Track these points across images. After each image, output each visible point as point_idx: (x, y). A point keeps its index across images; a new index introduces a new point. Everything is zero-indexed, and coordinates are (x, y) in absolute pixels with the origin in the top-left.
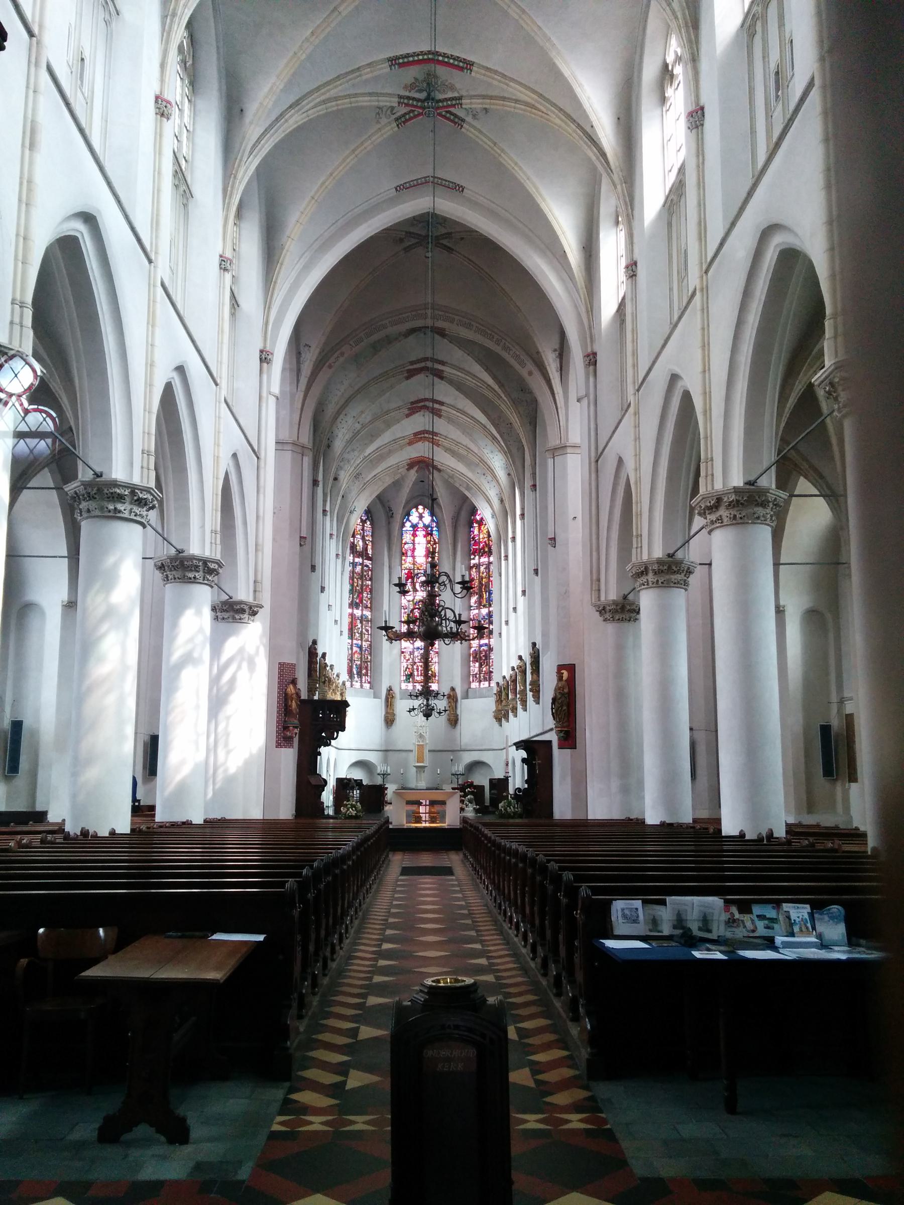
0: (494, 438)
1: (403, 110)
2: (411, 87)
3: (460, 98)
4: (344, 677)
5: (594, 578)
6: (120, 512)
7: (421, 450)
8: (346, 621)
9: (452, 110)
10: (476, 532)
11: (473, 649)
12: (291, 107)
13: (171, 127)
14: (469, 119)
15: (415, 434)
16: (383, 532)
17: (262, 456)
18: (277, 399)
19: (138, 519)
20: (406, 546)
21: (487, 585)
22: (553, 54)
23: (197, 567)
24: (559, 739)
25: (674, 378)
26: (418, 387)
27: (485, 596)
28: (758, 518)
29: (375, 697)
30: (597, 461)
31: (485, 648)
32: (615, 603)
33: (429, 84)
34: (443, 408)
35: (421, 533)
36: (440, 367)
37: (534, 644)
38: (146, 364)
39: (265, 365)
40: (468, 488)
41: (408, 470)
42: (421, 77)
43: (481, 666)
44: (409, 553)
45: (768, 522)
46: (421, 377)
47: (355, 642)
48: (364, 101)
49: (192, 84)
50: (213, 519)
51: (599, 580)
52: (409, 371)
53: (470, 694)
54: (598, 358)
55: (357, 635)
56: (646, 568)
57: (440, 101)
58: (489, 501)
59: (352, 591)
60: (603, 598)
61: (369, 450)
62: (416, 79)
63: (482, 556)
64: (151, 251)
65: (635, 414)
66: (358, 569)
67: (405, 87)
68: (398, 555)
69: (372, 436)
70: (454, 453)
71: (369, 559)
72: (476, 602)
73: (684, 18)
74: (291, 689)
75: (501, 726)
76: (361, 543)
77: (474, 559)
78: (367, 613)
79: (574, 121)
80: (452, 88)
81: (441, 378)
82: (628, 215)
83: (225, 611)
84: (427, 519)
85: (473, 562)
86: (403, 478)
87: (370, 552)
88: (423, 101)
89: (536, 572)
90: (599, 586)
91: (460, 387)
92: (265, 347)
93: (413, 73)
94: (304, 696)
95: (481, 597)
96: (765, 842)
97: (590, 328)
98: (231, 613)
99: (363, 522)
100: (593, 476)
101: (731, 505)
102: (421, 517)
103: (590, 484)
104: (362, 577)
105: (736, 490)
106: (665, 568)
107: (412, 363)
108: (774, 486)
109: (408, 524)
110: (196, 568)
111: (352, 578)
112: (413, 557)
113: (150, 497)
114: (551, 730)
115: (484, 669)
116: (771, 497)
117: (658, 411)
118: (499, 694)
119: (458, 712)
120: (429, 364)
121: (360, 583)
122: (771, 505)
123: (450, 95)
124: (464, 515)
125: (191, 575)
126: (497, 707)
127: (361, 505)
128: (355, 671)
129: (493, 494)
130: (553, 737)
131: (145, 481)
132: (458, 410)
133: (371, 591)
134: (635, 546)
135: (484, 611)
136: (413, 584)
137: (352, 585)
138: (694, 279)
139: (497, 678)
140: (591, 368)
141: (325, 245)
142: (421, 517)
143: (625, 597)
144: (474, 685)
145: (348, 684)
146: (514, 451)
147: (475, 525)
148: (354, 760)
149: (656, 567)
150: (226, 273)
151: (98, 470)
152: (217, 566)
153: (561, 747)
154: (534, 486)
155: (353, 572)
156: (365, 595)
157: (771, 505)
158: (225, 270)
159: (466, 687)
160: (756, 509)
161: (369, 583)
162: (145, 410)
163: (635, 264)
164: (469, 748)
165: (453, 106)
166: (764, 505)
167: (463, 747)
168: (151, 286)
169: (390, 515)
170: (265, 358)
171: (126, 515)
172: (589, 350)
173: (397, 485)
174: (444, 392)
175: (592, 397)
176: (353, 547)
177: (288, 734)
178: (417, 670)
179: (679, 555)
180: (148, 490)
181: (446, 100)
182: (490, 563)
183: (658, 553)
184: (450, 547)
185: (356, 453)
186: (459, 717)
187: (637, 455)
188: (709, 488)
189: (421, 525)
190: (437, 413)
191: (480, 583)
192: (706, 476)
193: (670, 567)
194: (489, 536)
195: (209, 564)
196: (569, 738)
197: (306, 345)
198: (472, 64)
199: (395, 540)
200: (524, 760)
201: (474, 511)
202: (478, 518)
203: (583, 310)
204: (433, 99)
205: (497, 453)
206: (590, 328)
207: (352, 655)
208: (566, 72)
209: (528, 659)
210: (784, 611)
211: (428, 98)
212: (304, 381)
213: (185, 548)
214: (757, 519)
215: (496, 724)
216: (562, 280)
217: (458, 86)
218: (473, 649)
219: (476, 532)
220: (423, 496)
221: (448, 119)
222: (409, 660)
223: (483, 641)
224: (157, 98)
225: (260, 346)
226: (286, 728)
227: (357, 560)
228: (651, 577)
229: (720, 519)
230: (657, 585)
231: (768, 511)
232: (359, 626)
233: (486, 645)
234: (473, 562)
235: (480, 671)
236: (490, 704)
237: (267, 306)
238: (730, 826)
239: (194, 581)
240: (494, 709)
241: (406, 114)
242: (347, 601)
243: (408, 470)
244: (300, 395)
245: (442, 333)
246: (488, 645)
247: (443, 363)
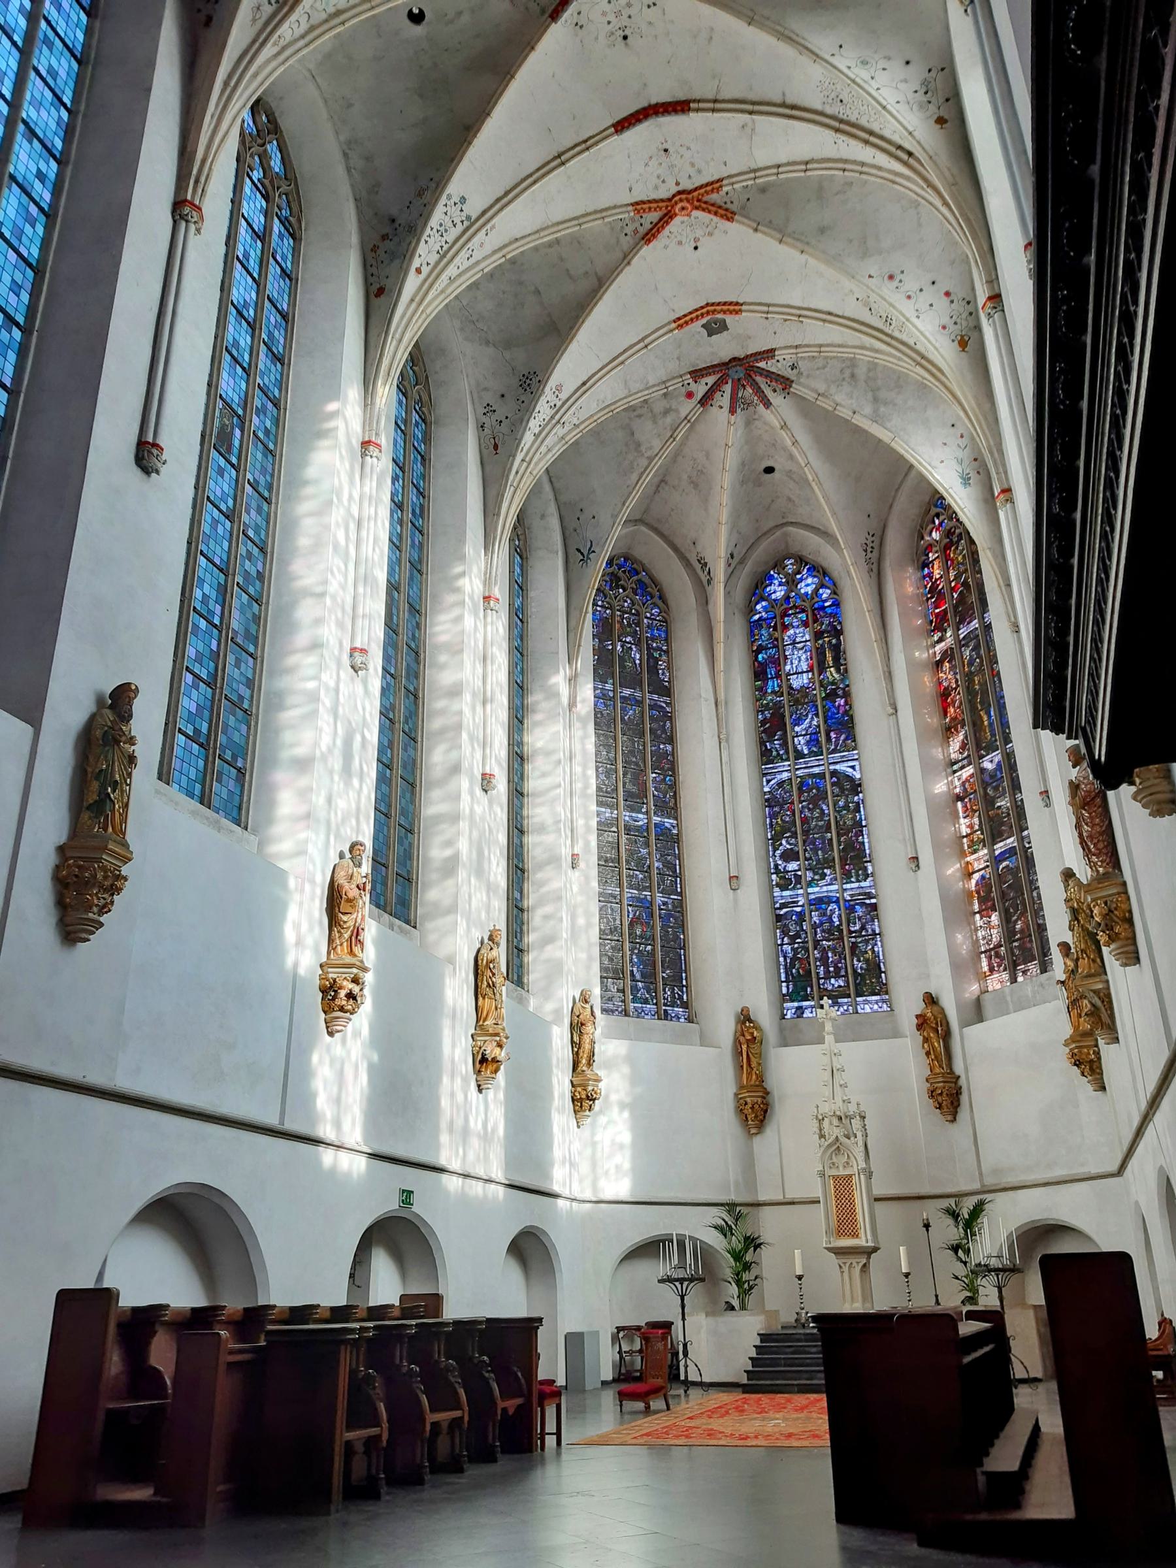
10: (937, 573)
11: (976, 876)
29: (704, 1041)
43: (1007, 919)
44: (771, 671)
63: (961, 622)
72: (963, 747)
75: (1103, 1088)
77: (941, 640)
115: (1018, 927)
119: (959, 1068)
126: (1076, 1028)
142: (792, 582)
148: (637, 1237)
164: (1011, 1180)
167: (990, 1181)
178: (824, 960)
186: (962, 1082)
205: (881, 65)
215: (1083, 1086)
218: (976, 876)
222: (797, 936)
223: (999, 848)
233: (1011, 852)
235: (1009, 932)
240: (1068, 1031)
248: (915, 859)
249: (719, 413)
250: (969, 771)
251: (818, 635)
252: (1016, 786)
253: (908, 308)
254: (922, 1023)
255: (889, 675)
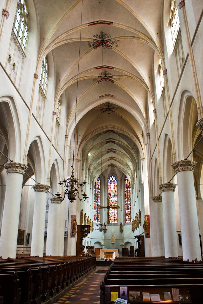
0: (129, 158)
1: (99, 79)
2: (101, 74)
3: (113, 76)
4: (93, 220)
5: (152, 190)
6: (16, 171)
7: (112, 162)
8: (94, 205)
9: (111, 79)
10: (126, 182)
12: (71, 79)
13: (38, 82)
14: (115, 81)
15: (110, 158)
16: (103, 183)
17: (65, 161)
18: (69, 147)
19: (22, 173)
20: (109, 186)
21: (130, 196)
22: (133, 64)
23: (43, 187)
24: (146, 235)
25: (166, 135)
26: (109, 146)
27: (129, 199)
28: (189, 169)
30: (151, 160)
31: (129, 212)
32: (157, 197)
33: (105, 74)
34: (116, 151)
35: (112, 183)
36: (114, 141)
37: (140, 210)
38: (27, 134)
39: (66, 139)
40: (124, 171)
41: (109, 167)
42: (103, 72)
43: (128, 217)
44: (110, 188)
45: (192, 170)
46: (110, 143)
47: (96, 211)
48: (90, 78)
49: (48, 75)
50: (48, 176)
51: (153, 191)
52: (106, 142)
53: (126, 224)
54: (150, 134)
55: (96, 209)
56: (163, 186)
57: (108, 77)
58: (129, 174)
59: (95, 198)
60: (154, 196)
61: (98, 162)
62: (102, 72)
64: (30, 107)
65: (158, 146)
66: (97, 192)
67: (99, 74)
68: (107, 189)
69: (99, 158)
70: (120, 163)
71: (99, 190)
73: (160, 51)
74: (74, 222)
76: (97, 186)
78: (99, 203)
79: (139, 78)
80: (111, 74)
81: (115, 143)
82: (153, 99)
83: (54, 200)
84: (114, 179)
85: (126, 190)
86: (107, 169)
87: (100, 188)
88: (104, 77)
89: (140, 191)
90: (153, 193)
91: (119, 145)
92: (66, 134)
93: (101, 71)
94: (79, 223)
95: (128, 199)
96: (194, 262)
97: (148, 127)
98: (56, 201)
99: (98, 180)
100: (150, 164)
101: (181, 165)
102: (112, 179)
103: (149, 166)
104: (98, 194)
105: (182, 161)
106: (168, 186)
107: (107, 140)
108: (193, 160)
109: (109, 181)
110: (43, 188)
111: (95, 195)
112: (111, 189)
113: (25, 167)
114: (144, 233)
116: (192, 163)
117: (163, 144)
118: (133, 224)
119: (123, 229)
120: (112, 140)
121: (97, 196)
122: (192, 165)
123: (110, 75)
124: (123, 178)
125: (41, 190)
127: (97, 176)
128: (96, 218)
129: (130, 172)
130: (144, 235)
131: (24, 163)
132: (119, 151)
133: (100, 198)
134: (160, 180)
135: (129, 203)
136: (111, 196)
137: (95, 196)
138: (168, 110)
139: (132, 220)
140: (148, 137)
141: (82, 110)
142: (112, 179)
143: (160, 195)
144: (127, 222)
145: (94, 222)
146: (134, 161)
147: (126, 181)
148: (95, 242)
149: (165, 186)
150: (54, 116)
151: (11, 160)
152: (48, 188)
153: (146, 237)
154: (138, 169)
155: (95, 193)
156: (98, 199)
157: (192, 165)
158: (54, 115)
159: (124, 222)
160: (188, 166)
161: (99, 196)
162: (25, 145)
163: (156, 109)
165: (111, 78)
166: (190, 165)
167: (124, 238)
168: (29, 115)
169: (105, 178)
170: (66, 137)
171: (18, 172)
172: (148, 133)
173: (106, 171)
174: (115, 147)
175: (149, 144)
176: (95, 187)
177: (74, 234)
179: (171, 182)
180: (24, 165)
181: (109, 77)
182: (130, 190)
183: (166, 182)
184: (120, 186)
185: (95, 163)
187: (159, 156)
188: (175, 161)
189: (113, 181)
190: (115, 152)
191: (128, 195)
192: (174, 158)
193: (169, 185)
194: (130, 183)
195: (46, 187)
196: (148, 235)
197: (80, 135)
198: (114, 68)
199: (106, 185)
200: (137, 241)
201: (126, 177)
202: (127, 179)
203: (145, 123)
204: (106, 77)
206: (148, 127)
207: (95, 214)
208: (136, 68)
209: (138, 214)
210: (202, 198)
211: (105, 76)
212: (79, 144)
213: (40, 183)
214: (188, 169)
215: (132, 232)
216: (140, 116)
217: (112, 74)
219: (126, 182)
220: (112, 173)
221: (110, 81)
224: (34, 74)
225: (65, 134)
226: (73, 232)
227: (96, 190)
228: (164, 188)
229: (178, 169)
230: (166, 191)
231: (192, 167)
232: (97, 207)
234: (126, 190)
235: (128, 218)
236: (130, 227)
237: (67, 125)
238: (185, 259)
239: (42, 191)
240: (132, 228)
241: (100, 80)
242: (94, 200)
243: (109, 167)
244: (78, 147)
245: (113, 132)
246: (130, 211)
247: (114, 139)
248: (121, 210)
249: (110, 167)
250: (127, 203)
251: (114, 185)
252: (131, 206)
253: (128, 170)
254: (120, 225)
255: (121, 192)
